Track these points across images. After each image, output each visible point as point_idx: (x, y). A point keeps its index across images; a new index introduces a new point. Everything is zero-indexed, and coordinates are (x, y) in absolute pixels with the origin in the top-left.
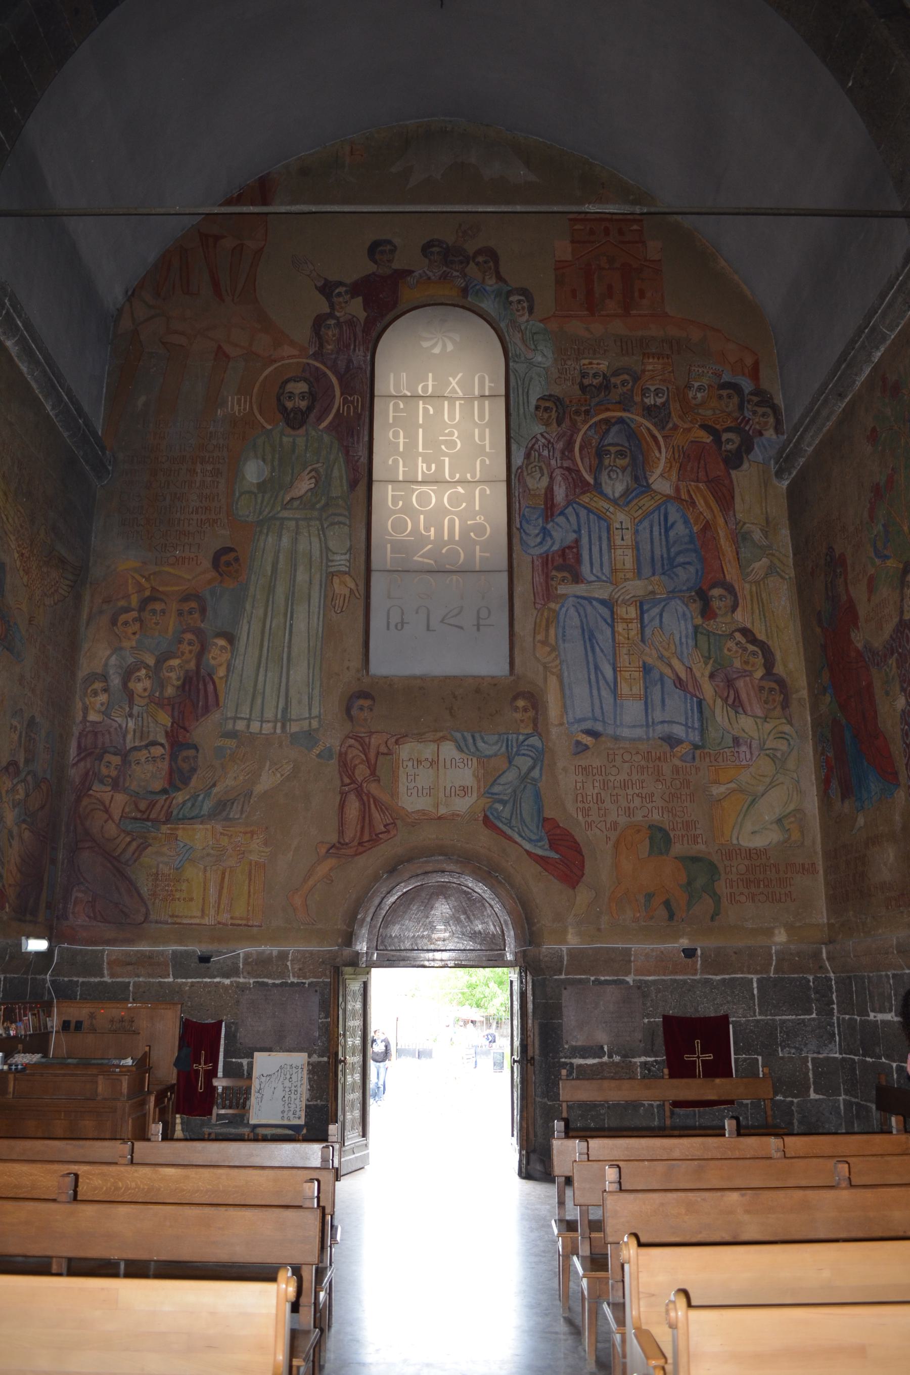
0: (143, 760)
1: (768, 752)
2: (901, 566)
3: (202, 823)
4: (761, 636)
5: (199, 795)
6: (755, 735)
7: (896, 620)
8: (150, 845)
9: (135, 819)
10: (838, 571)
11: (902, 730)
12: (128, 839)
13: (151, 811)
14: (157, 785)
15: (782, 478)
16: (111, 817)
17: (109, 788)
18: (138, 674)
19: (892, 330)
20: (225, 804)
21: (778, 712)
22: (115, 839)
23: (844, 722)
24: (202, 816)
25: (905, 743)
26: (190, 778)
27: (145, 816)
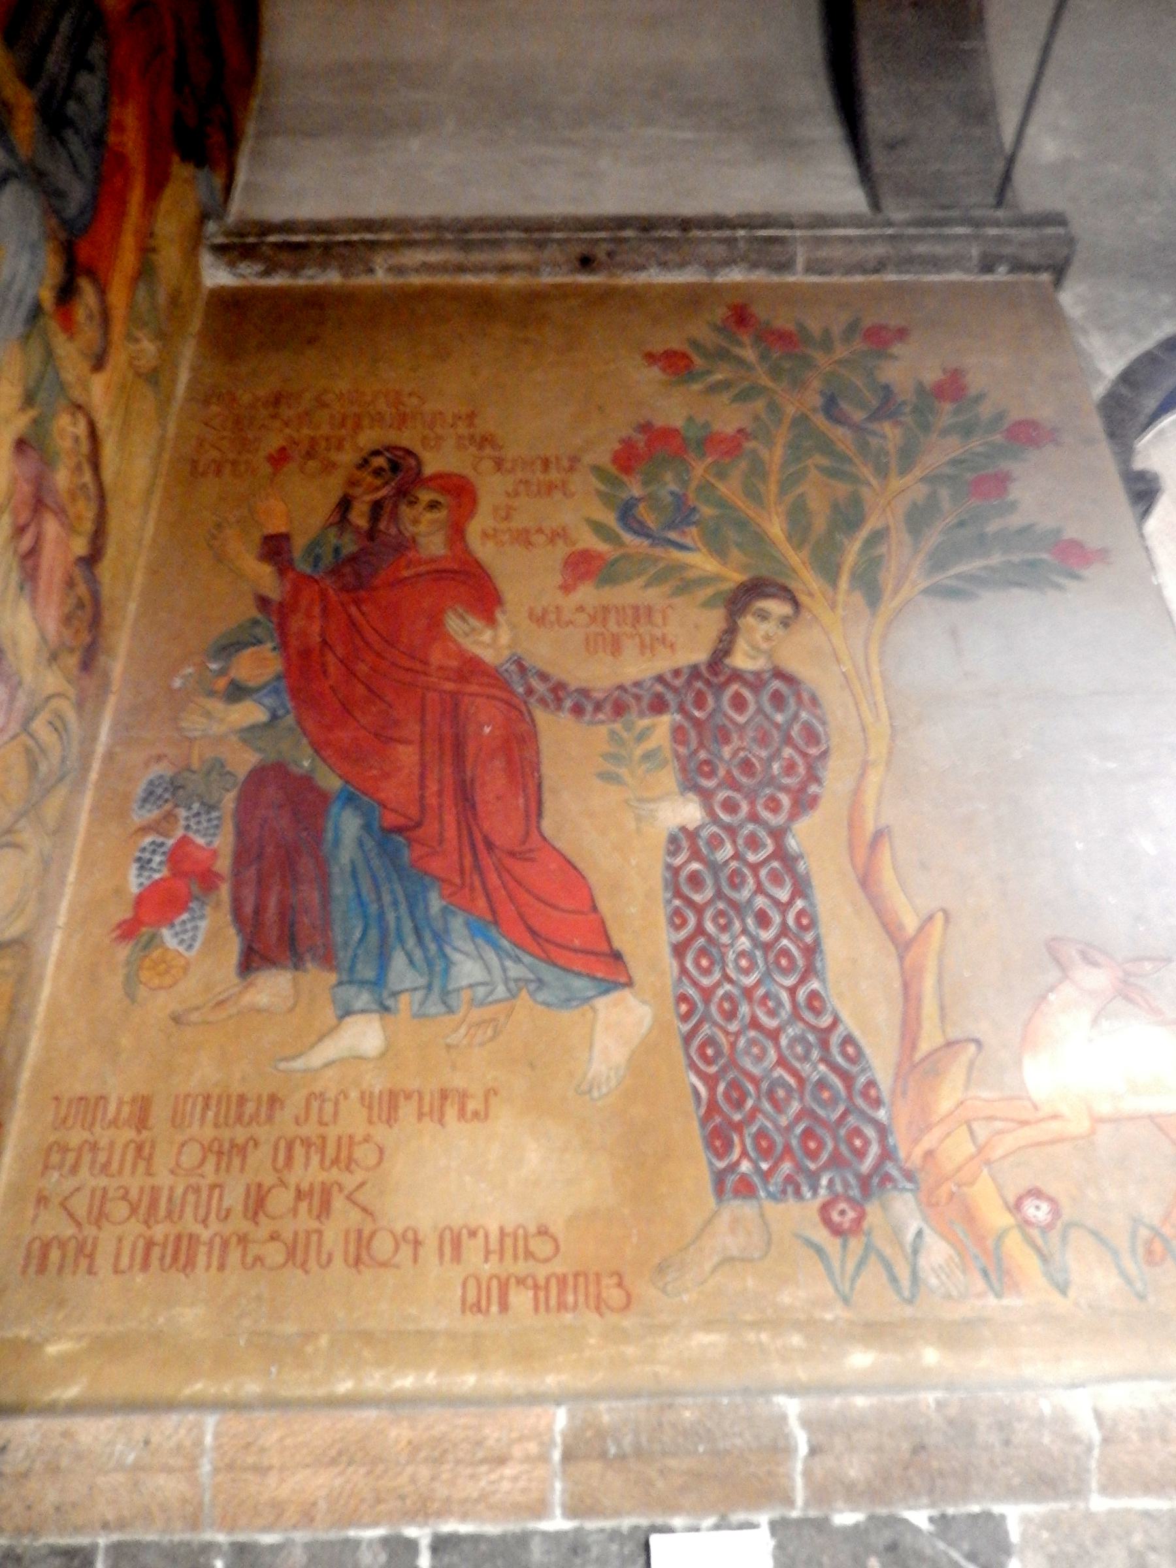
1: (30, 743)
2: (738, 577)
4: (108, 475)
6: (28, 676)
7: (700, 656)
10: (425, 496)
11: (676, 871)
15: (232, 264)
19: (809, 269)
21: (72, 661)
23: (331, 782)
25: (678, 893)
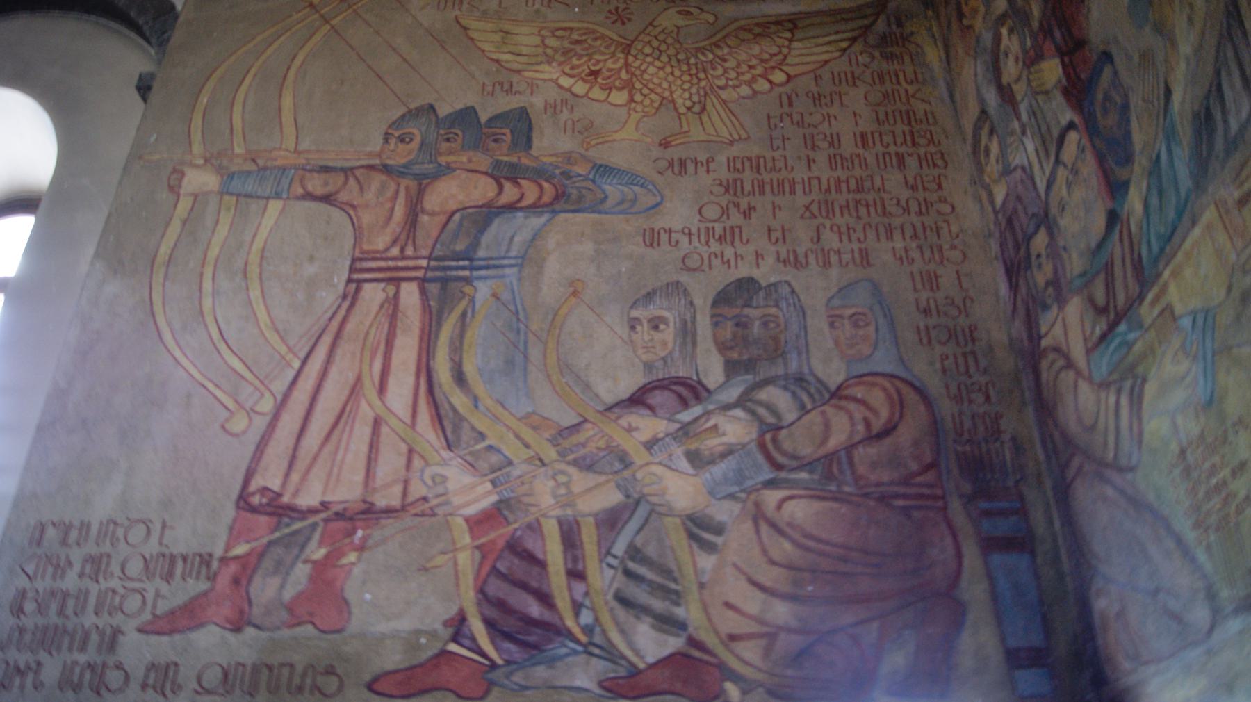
0: (1064, 192)
3: (1194, 223)
5: (1158, 156)
8: (1144, 380)
9: (1104, 337)
12: (1112, 399)
13: (1114, 295)
14: (1099, 222)
16: (1079, 373)
17: (1055, 309)
18: (1002, 47)
20: (1209, 115)
22: (1098, 413)
24: (1187, 201)
26: (1128, 135)
27: (1112, 316)
